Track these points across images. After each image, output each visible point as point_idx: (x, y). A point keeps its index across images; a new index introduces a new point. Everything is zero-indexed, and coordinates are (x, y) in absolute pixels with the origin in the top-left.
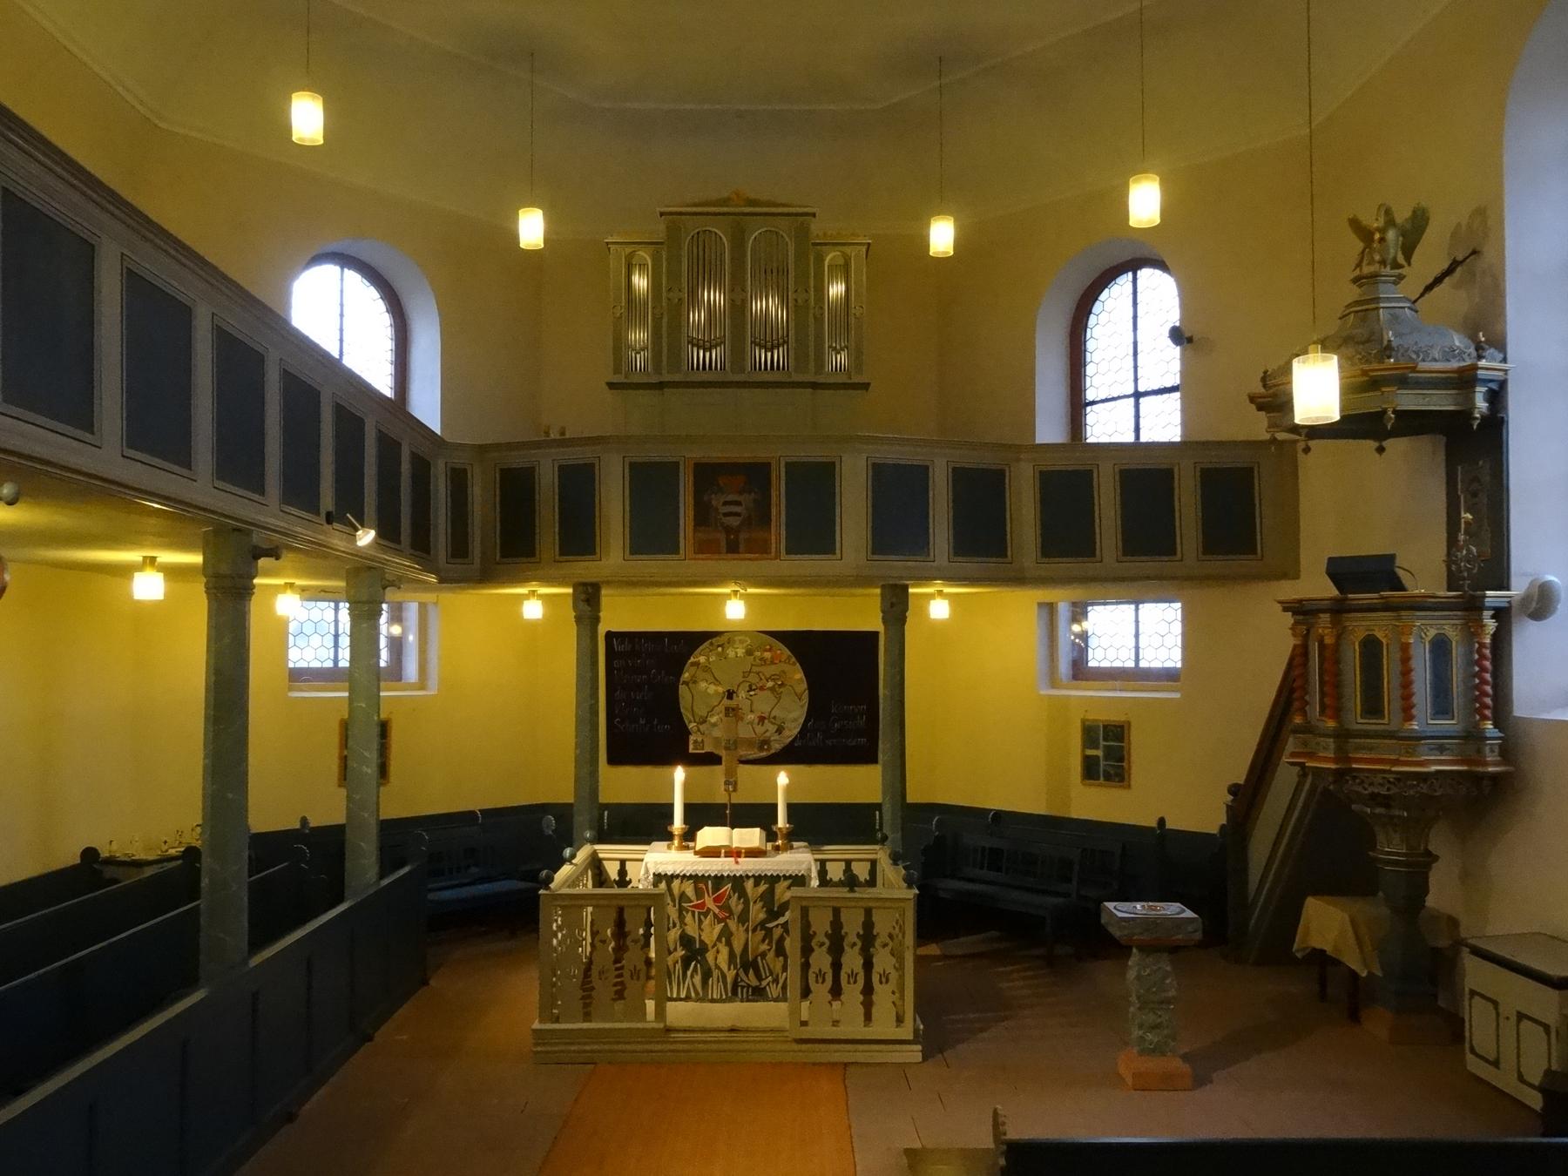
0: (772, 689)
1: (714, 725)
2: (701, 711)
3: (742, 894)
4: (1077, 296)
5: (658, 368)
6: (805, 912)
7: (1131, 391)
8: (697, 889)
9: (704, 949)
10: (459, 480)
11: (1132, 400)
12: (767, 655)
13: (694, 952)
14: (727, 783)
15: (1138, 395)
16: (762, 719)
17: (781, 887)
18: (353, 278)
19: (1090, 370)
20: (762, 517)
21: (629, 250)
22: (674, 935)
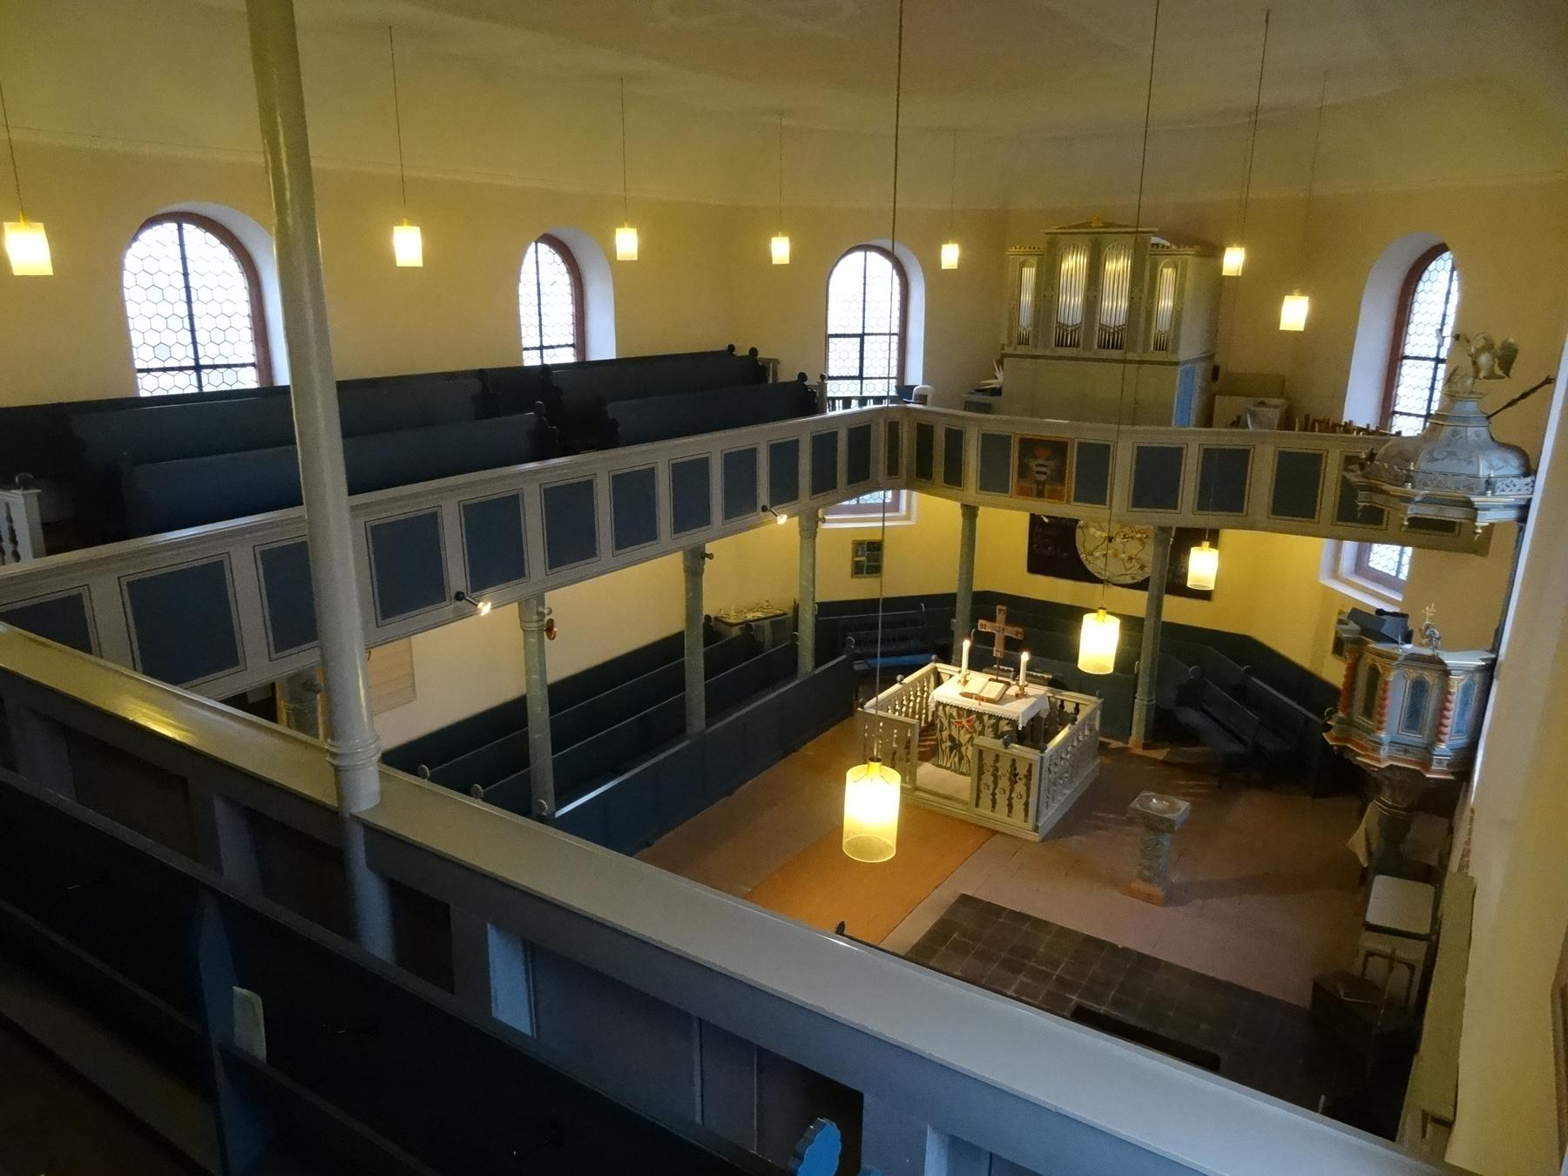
2: (1089, 547)
3: (982, 722)
6: (981, 752)
8: (959, 716)
9: (960, 745)
10: (893, 428)
13: (956, 745)
16: (1130, 559)
17: (1003, 723)
18: (874, 257)
19: (1412, 329)
20: (1060, 476)
22: (945, 734)
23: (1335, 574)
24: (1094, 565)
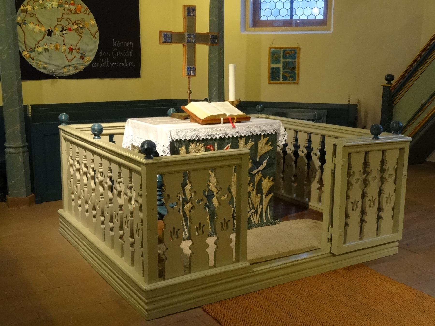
0: (76, 30)
1: (40, 53)
2: (31, 43)
12: (72, 7)
14: (189, 70)
16: (71, 50)
23: (246, 30)
24: (38, 62)
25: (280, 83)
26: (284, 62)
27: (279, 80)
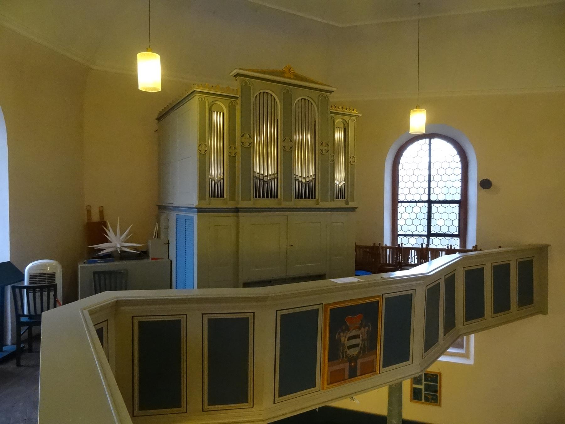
4: (399, 146)
5: (233, 197)
7: (426, 198)
11: (426, 204)
15: (430, 202)
21: (211, 99)
25: (423, 403)
26: (425, 384)
27: (421, 400)
